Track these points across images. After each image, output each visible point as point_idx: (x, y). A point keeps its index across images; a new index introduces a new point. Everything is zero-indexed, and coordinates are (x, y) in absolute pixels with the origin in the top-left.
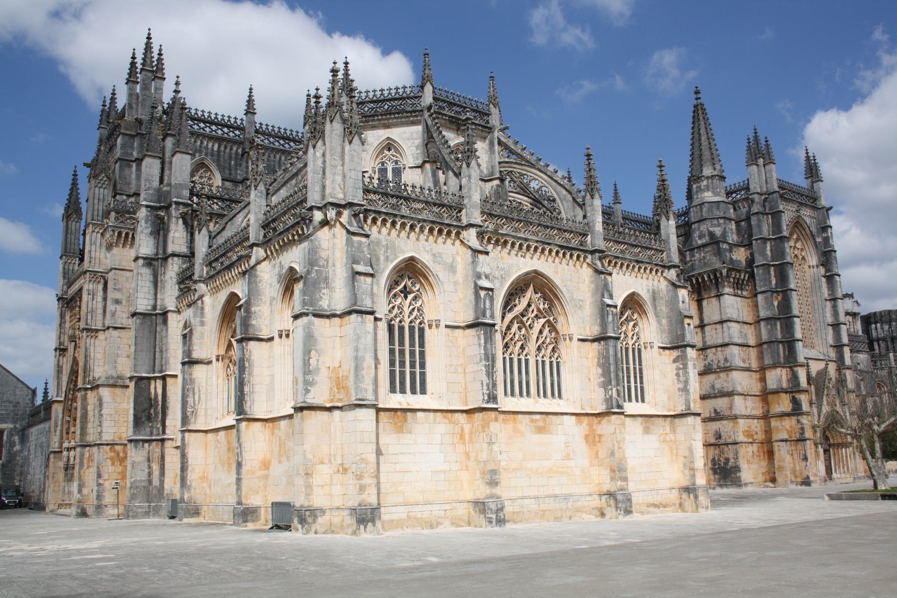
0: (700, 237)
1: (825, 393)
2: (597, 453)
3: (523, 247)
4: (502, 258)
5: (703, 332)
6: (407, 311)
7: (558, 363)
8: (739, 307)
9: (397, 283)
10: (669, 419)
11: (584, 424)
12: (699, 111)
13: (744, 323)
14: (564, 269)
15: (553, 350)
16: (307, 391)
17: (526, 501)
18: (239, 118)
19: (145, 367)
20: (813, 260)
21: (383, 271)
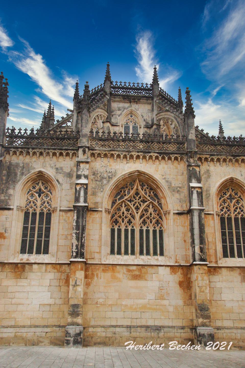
2: (191, 296)
4: (110, 165)
6: (39, 203)
7: (161, 232)
11: (179, 273)
14: (164, 168)
15: (157, 222)
17: (118, 329)
21: (19, 181)
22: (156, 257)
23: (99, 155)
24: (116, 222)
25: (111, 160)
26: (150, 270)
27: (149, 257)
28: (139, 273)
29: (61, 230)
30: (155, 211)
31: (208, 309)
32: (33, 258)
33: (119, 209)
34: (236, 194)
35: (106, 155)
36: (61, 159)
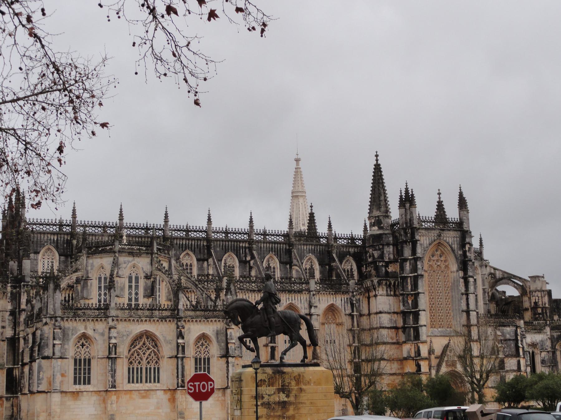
0: (370, 257)
1: (446, 359)
3: (140, 320)
5: (370, 318)
6: (83, 353)
7: (158, 369)
8: (391, 302)
9: (79, 342)
10: (221, 391)
12: (377, 169)
13: (394, 313)
15: (156, 362)
16: (38, 387)
18: (68, 220)
19: (11, 363)
20: (454, 266)
22: (155, 384)
23: (121, 320)
24: (131, 363)
25: (128, 323)
26: (152, 393)
27: (151, 384)
28: (146, 394)
29: (98, 370)
30: (155, 355)
31: (183, 414)
32: (82, 387)
33: (133, 355)
34: (206, 342)
35: (125, 320)
36: (96, 323)
